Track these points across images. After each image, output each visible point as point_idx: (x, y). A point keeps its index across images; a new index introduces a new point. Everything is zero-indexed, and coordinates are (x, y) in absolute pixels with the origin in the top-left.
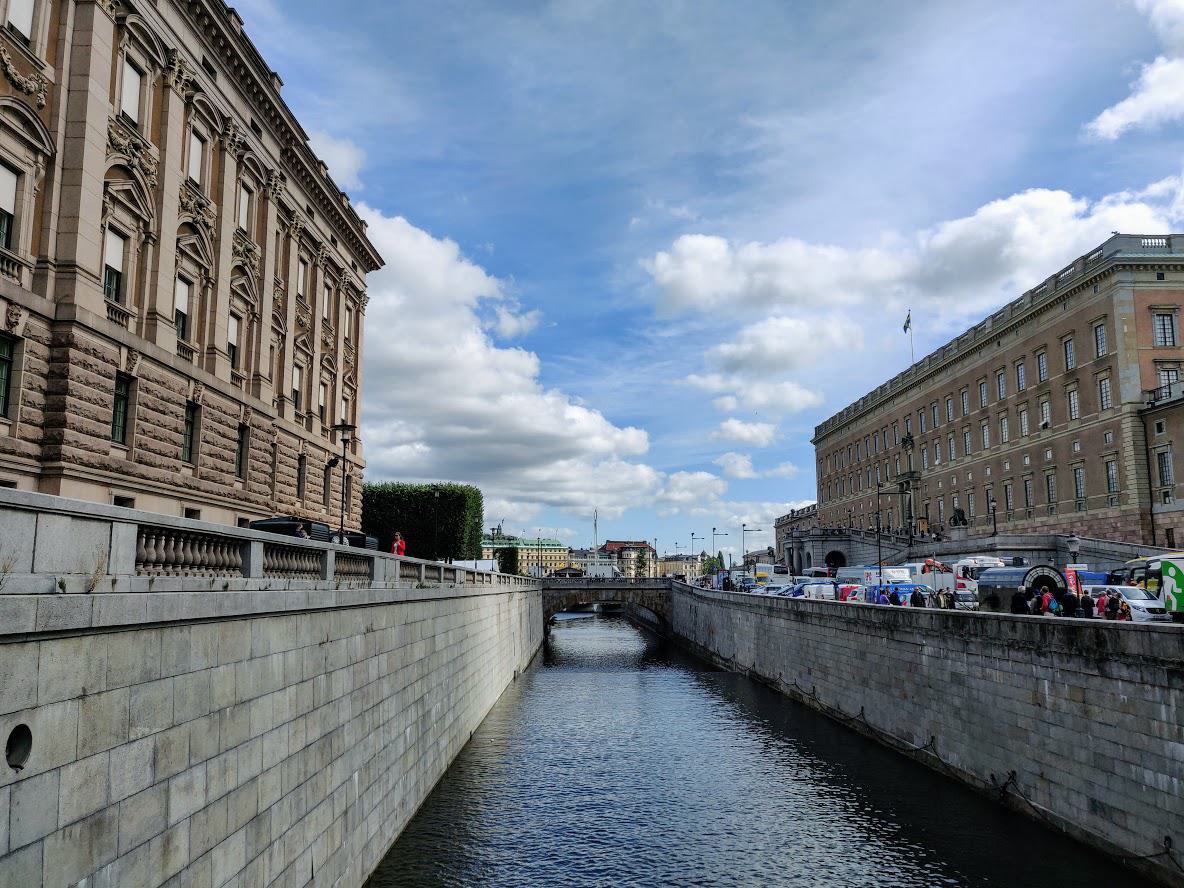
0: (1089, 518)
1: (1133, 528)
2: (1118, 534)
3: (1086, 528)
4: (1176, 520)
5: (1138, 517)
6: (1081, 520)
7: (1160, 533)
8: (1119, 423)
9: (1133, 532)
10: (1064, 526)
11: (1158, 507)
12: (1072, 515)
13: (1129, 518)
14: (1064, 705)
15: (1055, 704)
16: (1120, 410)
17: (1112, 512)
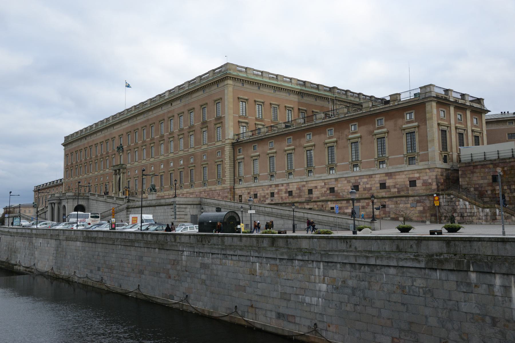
0: (208, 190)
1: (226, 195)
2: (220, 197)
3: (206, 195)
4: (243, 192)
5: (229, 190)
6: (205, 191)
7: (237, 197)
8: (224, 147)
9: (227, 197)
10: (197, 193)
11: (237, 186)
12: (201, 188)
13: (225, 191)
14: (266, 273)
15: (261, 273)
16: (225, 142)
17: (218, 187)
